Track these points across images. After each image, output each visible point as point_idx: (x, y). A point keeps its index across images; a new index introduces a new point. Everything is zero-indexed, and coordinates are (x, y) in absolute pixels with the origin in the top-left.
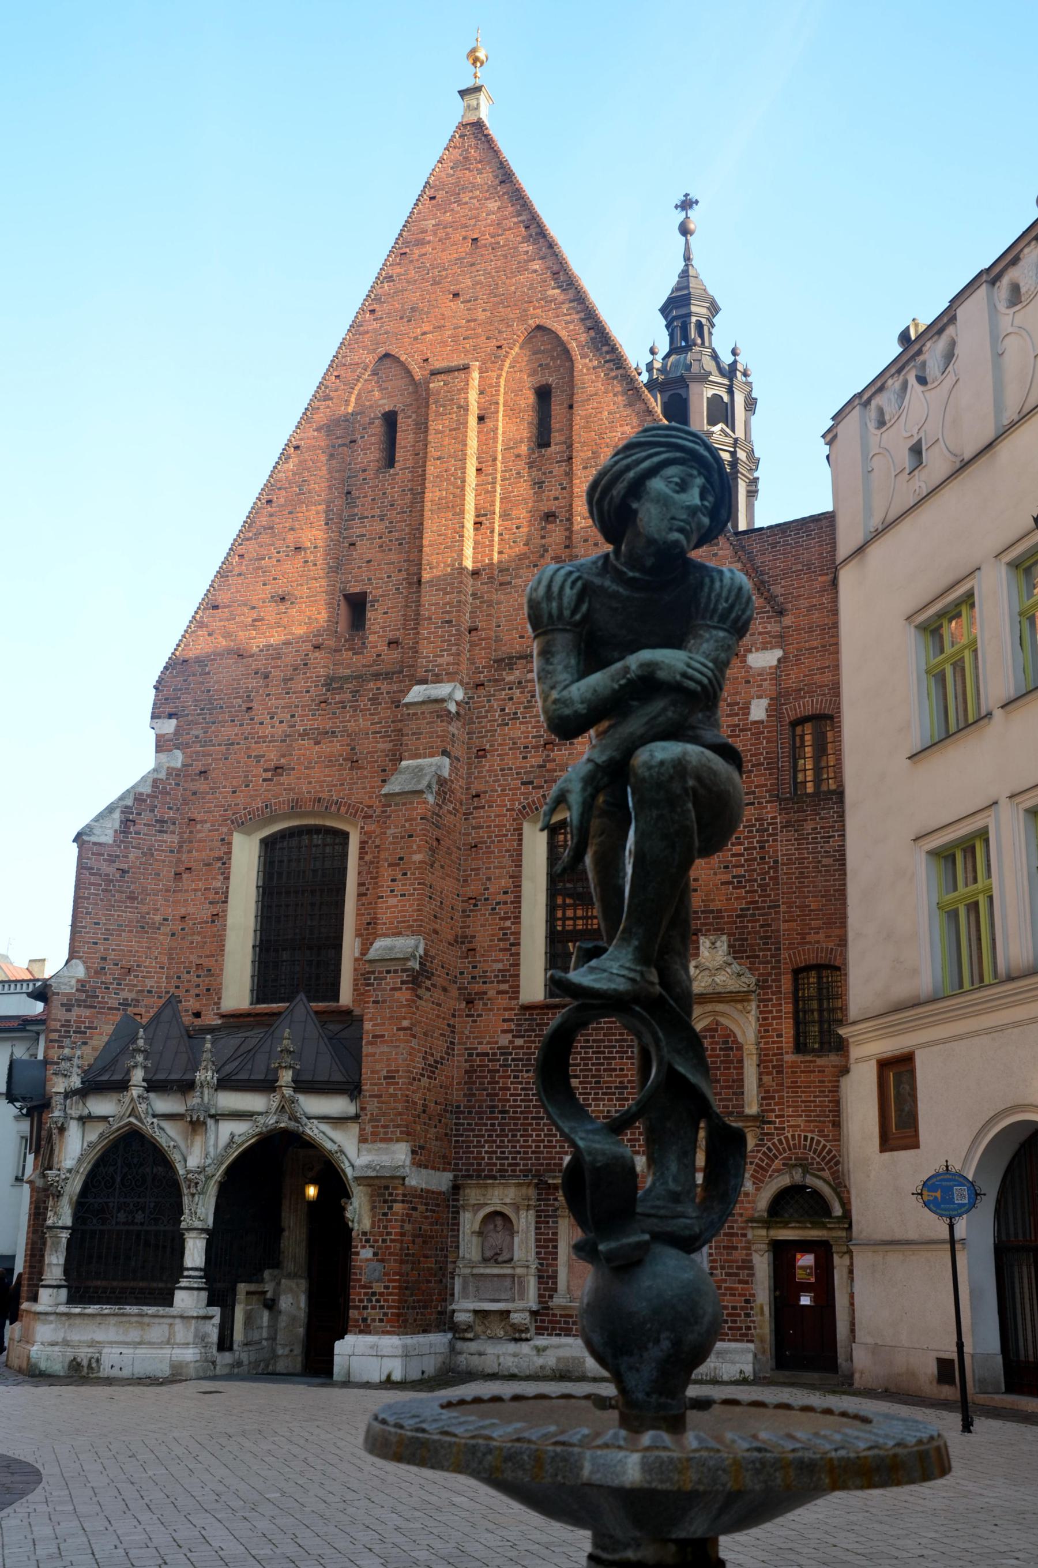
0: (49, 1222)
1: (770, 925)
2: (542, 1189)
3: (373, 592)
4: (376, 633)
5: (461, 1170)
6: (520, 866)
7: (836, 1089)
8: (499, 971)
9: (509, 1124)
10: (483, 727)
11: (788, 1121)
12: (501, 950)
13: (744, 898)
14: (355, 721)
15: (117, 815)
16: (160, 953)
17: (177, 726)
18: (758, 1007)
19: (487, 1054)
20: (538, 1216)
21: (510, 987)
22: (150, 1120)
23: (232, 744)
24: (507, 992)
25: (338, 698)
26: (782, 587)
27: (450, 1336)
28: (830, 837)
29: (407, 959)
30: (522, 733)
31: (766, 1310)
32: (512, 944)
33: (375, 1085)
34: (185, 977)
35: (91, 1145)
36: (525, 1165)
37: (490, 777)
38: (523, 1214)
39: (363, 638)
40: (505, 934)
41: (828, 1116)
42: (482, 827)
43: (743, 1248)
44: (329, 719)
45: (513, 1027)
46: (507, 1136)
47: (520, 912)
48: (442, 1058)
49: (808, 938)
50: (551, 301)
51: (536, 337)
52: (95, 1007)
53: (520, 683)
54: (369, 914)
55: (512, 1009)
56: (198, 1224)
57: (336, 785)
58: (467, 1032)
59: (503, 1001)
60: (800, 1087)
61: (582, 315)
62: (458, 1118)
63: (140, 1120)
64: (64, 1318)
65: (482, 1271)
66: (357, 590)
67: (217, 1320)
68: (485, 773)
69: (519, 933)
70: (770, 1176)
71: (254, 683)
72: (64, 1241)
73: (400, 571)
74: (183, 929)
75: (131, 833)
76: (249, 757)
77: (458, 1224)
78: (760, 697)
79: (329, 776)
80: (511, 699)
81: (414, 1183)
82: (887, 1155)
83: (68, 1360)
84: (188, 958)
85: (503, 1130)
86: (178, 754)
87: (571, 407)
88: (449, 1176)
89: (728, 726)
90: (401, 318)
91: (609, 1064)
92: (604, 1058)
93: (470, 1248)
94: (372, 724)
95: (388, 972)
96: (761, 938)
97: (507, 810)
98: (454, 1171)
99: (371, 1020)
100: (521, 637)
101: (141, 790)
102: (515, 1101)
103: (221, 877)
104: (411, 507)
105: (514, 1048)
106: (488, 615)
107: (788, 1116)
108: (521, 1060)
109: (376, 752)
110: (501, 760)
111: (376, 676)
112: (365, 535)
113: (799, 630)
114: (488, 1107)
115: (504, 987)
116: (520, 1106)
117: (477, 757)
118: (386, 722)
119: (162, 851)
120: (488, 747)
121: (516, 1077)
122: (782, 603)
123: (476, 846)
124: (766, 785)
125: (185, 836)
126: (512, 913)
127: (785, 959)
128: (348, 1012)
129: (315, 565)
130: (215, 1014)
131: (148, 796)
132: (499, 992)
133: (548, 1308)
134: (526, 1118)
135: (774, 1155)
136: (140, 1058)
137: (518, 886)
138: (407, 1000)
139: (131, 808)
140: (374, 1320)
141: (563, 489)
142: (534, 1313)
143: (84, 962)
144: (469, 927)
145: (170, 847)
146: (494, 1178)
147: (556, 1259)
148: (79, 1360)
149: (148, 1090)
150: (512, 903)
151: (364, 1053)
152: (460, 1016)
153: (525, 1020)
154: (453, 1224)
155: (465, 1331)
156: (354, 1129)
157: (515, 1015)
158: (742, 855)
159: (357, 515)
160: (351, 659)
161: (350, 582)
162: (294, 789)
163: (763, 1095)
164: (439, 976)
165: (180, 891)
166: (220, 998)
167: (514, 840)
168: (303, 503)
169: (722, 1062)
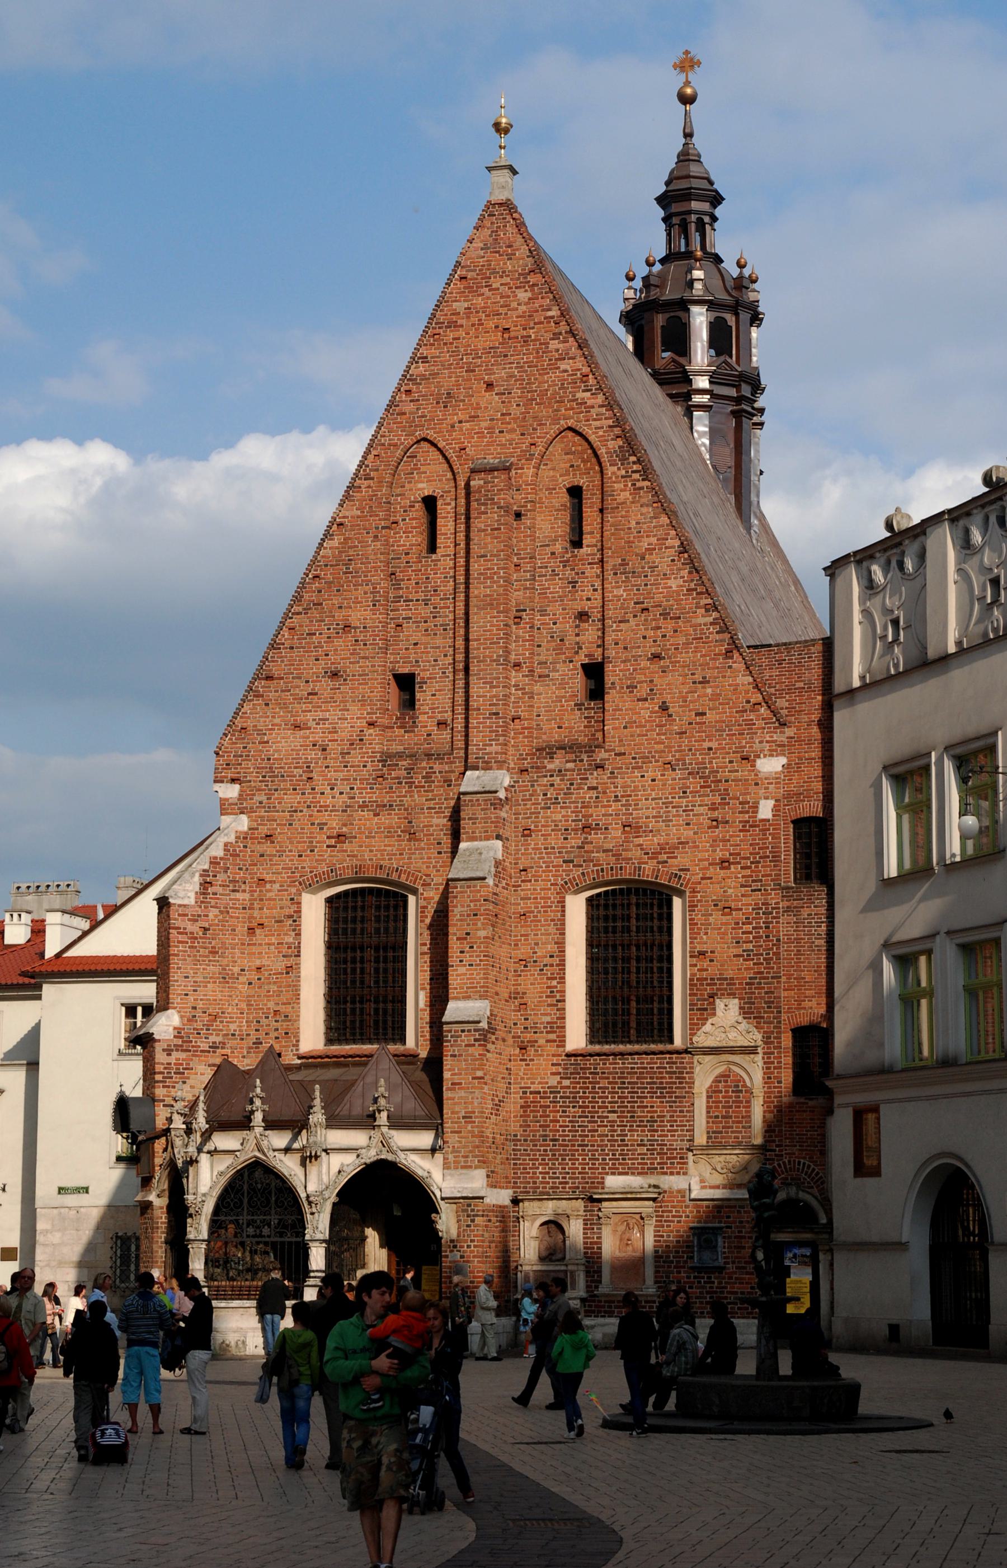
1: (773, 993)
3: (421, 675)
4: (425, 713)
5: (519, 1188)
6: (564, 934)
7: (823, 1125)
8: (548, 1023)
9: (559, 1150)
12: (549, 1005)
13: (752, 969)
15: (197, 879)
17: (241, 791)
18: (763, 1058)
19: (539, 1093)
20: (585, 1224)
21: (558, 1037)
23: (296, 811)
24: (555, 1041)
25: (394, 774)
32: (559, 1002)
33: (456, 1123)
35: (221, 1174)
37: (535, 854)
38: (573, 1222)
39: (414, 718)
40: (552, 992)
42: (530, 899)
44: (387, 793)
45: (561, 1070)
46: (557, 1159)
48: (503, 1097)
50: (581, 404)
51: (567, 437)
53: (560, 771)
55: (560, 1056)
56: (319, 1236)
57: (395, 854)
59: (551, 1048)
66: (406, 671)
68: (530, 851)
69: (564, 992)
71: (312, 755)
74: (259, 979)
76: (313, 824)
78: (766, 798)
79: (389, 846)
80: (552, 785)
82: (859, 1180)
86: (244, 818)
89: (740, 822)
90: (438, 403)
94: (427, 800)
95: (463, 1031)
96: (766, 1003)
99: (449, 1070)
100: (560, 727)
103: (293, 934)
105: (562, 1088)
108: (569, 1097)
109: (432, 826)
110: (545, 840)
111: (429, 755)
112: (410, 618)
115: (552, 1036)
116: (568, 1136)
117: (524, 836)
118: (440, 799)
120: (532, 827)
121: (563, 1112)
124: (771, 875)
129: (365, 645)
130: (294, 1055)
131: (221, 859)
132: (548, 1041)
133: (595, 1296)
134: (574, 1145)
136: (258, 1102)
139: (208, 871)
141: (595, 590)
142: (583, 1300)
143: (179, 1012)
150: (557, 965)
159: (402, 597)
161: (398, 662)
162: (356, 856)
165: (255, 944)
166: (298, 1041)
168: (351, 582)
169: (733, 1102)
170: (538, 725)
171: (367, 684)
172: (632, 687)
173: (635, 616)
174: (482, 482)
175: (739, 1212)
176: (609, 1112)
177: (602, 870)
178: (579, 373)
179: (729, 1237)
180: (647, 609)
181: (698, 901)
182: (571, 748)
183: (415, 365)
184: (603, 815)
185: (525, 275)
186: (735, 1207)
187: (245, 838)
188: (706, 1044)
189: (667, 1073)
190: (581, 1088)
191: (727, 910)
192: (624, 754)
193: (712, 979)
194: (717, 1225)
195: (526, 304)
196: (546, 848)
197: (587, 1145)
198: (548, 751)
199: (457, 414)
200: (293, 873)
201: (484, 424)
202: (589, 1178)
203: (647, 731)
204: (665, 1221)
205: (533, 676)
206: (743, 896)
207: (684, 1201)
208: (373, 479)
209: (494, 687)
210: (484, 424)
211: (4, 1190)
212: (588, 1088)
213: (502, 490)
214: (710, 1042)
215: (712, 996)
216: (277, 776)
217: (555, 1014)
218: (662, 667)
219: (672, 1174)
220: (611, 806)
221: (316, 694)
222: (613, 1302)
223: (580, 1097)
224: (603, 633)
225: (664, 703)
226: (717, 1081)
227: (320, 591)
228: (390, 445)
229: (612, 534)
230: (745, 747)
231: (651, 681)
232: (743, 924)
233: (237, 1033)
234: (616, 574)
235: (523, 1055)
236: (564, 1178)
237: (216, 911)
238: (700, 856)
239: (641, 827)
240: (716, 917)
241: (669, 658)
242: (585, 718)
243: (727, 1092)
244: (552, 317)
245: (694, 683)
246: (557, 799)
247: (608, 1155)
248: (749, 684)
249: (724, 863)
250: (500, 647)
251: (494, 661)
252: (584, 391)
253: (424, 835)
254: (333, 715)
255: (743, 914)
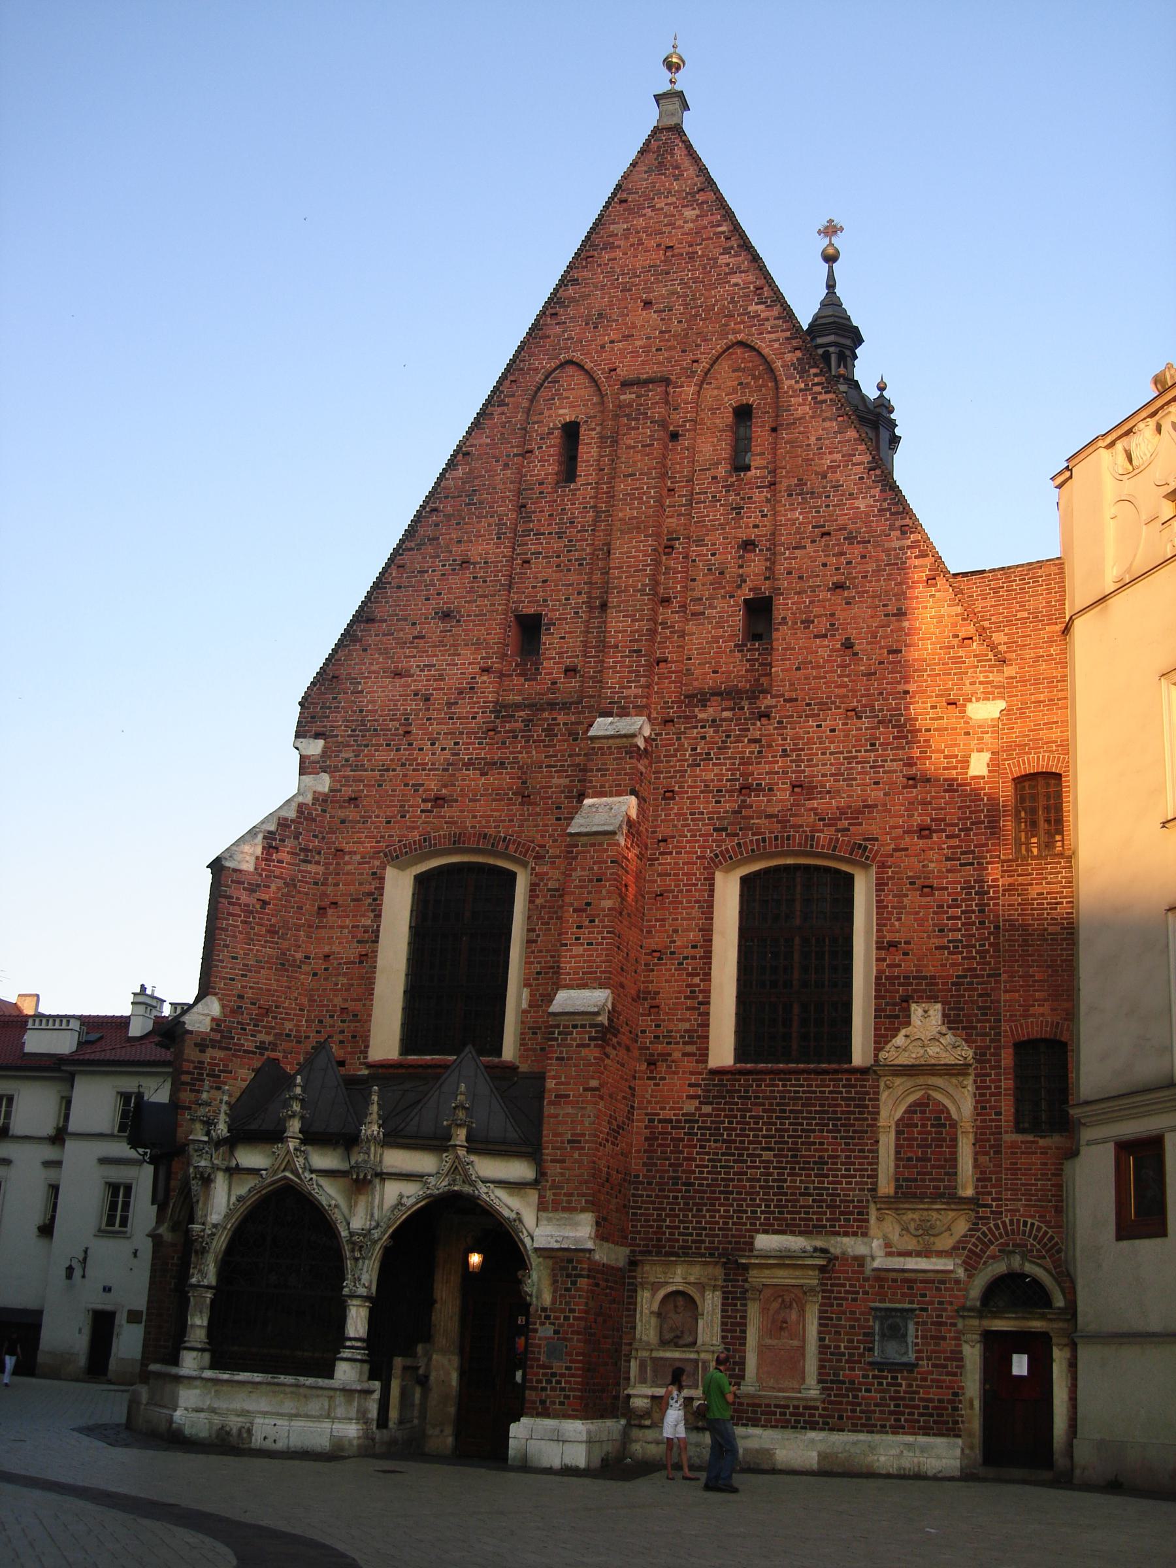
0: (194, 1280)
1: (989, 995)
2: (730, 1269)
3: (549, 614)
5: (639, 1245)
6: (712, 919)
7: (1059, 1173)
8: (686, 1031)
9: (693, 1198)
10: (672, 767)
11: (1007, 1205)
12: (687, 1009)
14: (527, 753)
16: (300, 994)
17: (325, 747)
18: (975, 1082)
19: (671, 1121)
20: (724, 1298)
21: (698, 1049)
22: (307, 1175)
23: (387, 770)
24: (694, 1055)
26: (1005, 634)
27: (623, 1422)
28: (1057, 903)
29: (597, 1014)
30: (715, 775)
31: (977, 1404)
32: (701, 1003)
34: (328, 1021)
35: (240, 1199)
36: (712, 1242)
37: (678, 820)
38: (709, 1295)
39: (537, 663)
40: (693, 992)
41: (1050, 1201)
43: (952, 1339)
46: (691, 1210)
47: (710, 969)
48: (624, 1123)
49: (1032, 1010)
50: (753, 317)
52: (230, 1049)
53: (714, 721)
54: (539, 963)
55: (700, 1073)
56: (362, 1291)
57: (504, 821)
58: (648, 1096)
59: (689, 1064)
60: (1020, 1169)
61: (788, 334)
62: (636, 1189)
63: (298, 1176)
64: (209, 1384)
65: (661, 1354)
66: (532, 611)
67: (376, 1396)
69: (709, 991)
70: (985, 1263)
72: (208, 1301)
73: (579, 593)
74: (326, 969)
75: (274, 861)
76: (406, 785)
77: (635, 1304)
78: (980, 750)
79: (497, 810)
80: (703, 738)
81: (597, 1257)
83: (215, 1428)
84: (331, 1001)
85: (687, 1204)
87: (774, 430)
88: (626, 1251)
90: (587, 324)
91: (808, 1137)
92: (802, 1130)
93: (646, 1329)
95: (575, 1026)
96: (979, 1008)
97: (697, 858)
98: (630, 1245)
99: (554, 1078)
100: (714, 672)
101: (284, 814)
102: (702, 1172)
103: (372, 915)
104: (595, 525)
106: (678, 647)
107: (1007, 1200)
108: (709, 1129)
109: (551, 787)
110: (691, 803)
111: (552, 705)
112: (540, 553)
113: (1023, 681)
114: (669, 1178)
115: (691, 1049)
116: (706, 1179)
117: (664, 798)
118: (563, 756)
119: (307, 882)
120: (676, 789)
121: (702, 1147)
122: (1006, 652)
123: (661, 895)
125: (331, 868)
126: (701, 969)
127: (1006, 1031)
128: (511, 1068)
129: (485, 582)
131: (292, 821)
132: (684, 1055)
134: (713, 1192)
135: (990, 1240)
136: (296, 1107)
137: (709, 941)
138: (595, 1058)
140: (554, 1403)
143: (220, 1000)
144: (652, 982)
145: (314, 878)
146: (677, 1255)
147: (744, 1344)
148: (228, 1429)
149: (304, 1142)
150: (701, 958)
151: (546, 1113)
152: (641, 1078)
153: (714, 1085)
154: (630, 1303)
155: (641, 1417)
156: (533, 1196)
157: (703, 1080)
158: (959, 918)
159: (532, 530)
160: (523, 685)
161: (523, 602)
162: (456, 823)
163: (978, 1176)
164: (624, 1034)
165: (325, 927)
166: (367, 1047)
167: (704, 891)
168: (474, 513)
170: (687, 670)
171: (484, 625)
172: (807, 622)
173: (813, 541)
174: (633, 396)
175: (939, 1289)
176: (763, 1149)
177: (764, 840)
178: (752, 286)
179: (924, 1323)
180: (829, 534)
181: (889, 878)
182: (731, 695)
183: (563, 288)
184: (767, 773)
185: (693, 194)
186: (933, 1282)
187: (325, 801)
188: (896, 1062)
189: (843, 1099)
190: (725, 1116)
191: (928, 889)
192: (796, 700)
193: (906, 978)
194: (907, 1306)
195: (693, 221)
196: (694, 814)
197: (732, 1193)
198: (701, 699)
199: (609, 334)
200: (377, 842)
201: (638, 343)
202: (733, 1236)
203: (826, 672)
204: (835, 1298)
205: (685, 613)
206: (948, 871)
207: (862, 1272)
208: (507, 405)
209: (637, 620)
210: (638, 343)
211: (135, 1254)
212: (736, 1117)
213: (657, 403)
214: (904, 1059)
215: (906, 1000)
216: (369, 730)
217: (696, 1020)
218: (846, 598)
219: (846, 1234)
220: (777, 762)
221: (423, 637)
222: (760, 1406)
223: (725, 1129)
224: (773, 563)
225: (848, 639)
226: (910, 1110)
227: (437, 525)
228: (529, 369)
229: (788, 452)
230: (952, 690)
231: (832, 615)
232: (949, 907)
233: (294, 1033)
234: (790, 495)
235: (652, 1072)
236: (700, 1235)
237: (280, 883)
238: (892, 822)
239: (816, 787)
240: (913, 899)
241: (855, 587)
242: (748, 660)
243: (924, 1126)
244: (723, 233)
245: (887, 615)
246: (709, 754)
247: (760, 1206)
248: (957, 615)
249: (924, 831)
250: (647, 575)
251: (639, 591)
252: (757, 304)
253: (542, 798)
254: (440, 660)
255: (949, 894)
